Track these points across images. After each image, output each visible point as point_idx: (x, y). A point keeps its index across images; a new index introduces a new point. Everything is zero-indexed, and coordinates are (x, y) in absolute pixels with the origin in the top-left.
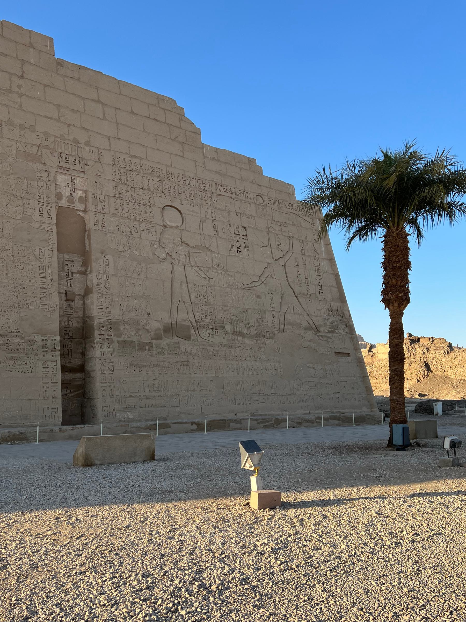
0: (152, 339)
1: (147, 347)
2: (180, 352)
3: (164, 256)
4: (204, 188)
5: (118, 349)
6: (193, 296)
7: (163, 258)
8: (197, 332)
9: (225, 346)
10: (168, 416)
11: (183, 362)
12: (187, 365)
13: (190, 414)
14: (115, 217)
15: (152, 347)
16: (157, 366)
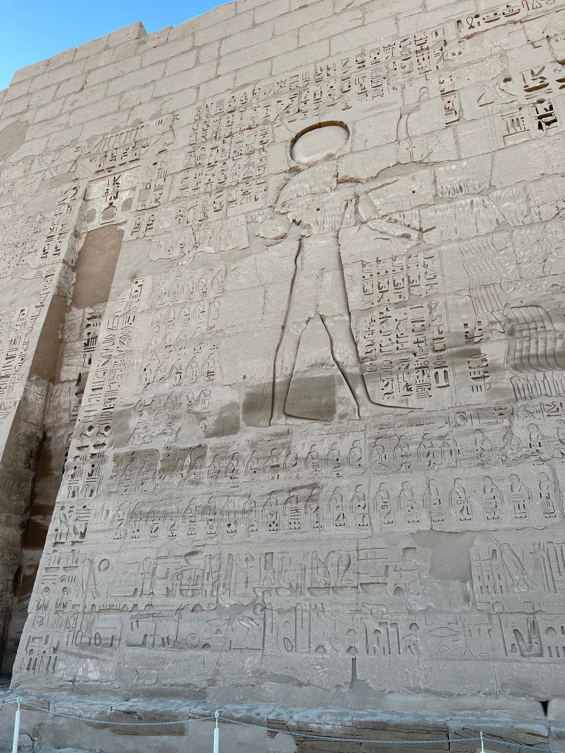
0: (209, 436)
1: (188, 460)
2: (290, 461)
3: (281, 230)
4: (419, 48)
5: (111, 477)
6: (355, 296)
7: (279, 234)
8: (359, 391)
9: (479, 414)
10: (212, 682)
11: (294, 489)
12: (310, 498)
13: (300, 684)
14: (178, 202)
15: (202, 457)
16: (205, 510)
